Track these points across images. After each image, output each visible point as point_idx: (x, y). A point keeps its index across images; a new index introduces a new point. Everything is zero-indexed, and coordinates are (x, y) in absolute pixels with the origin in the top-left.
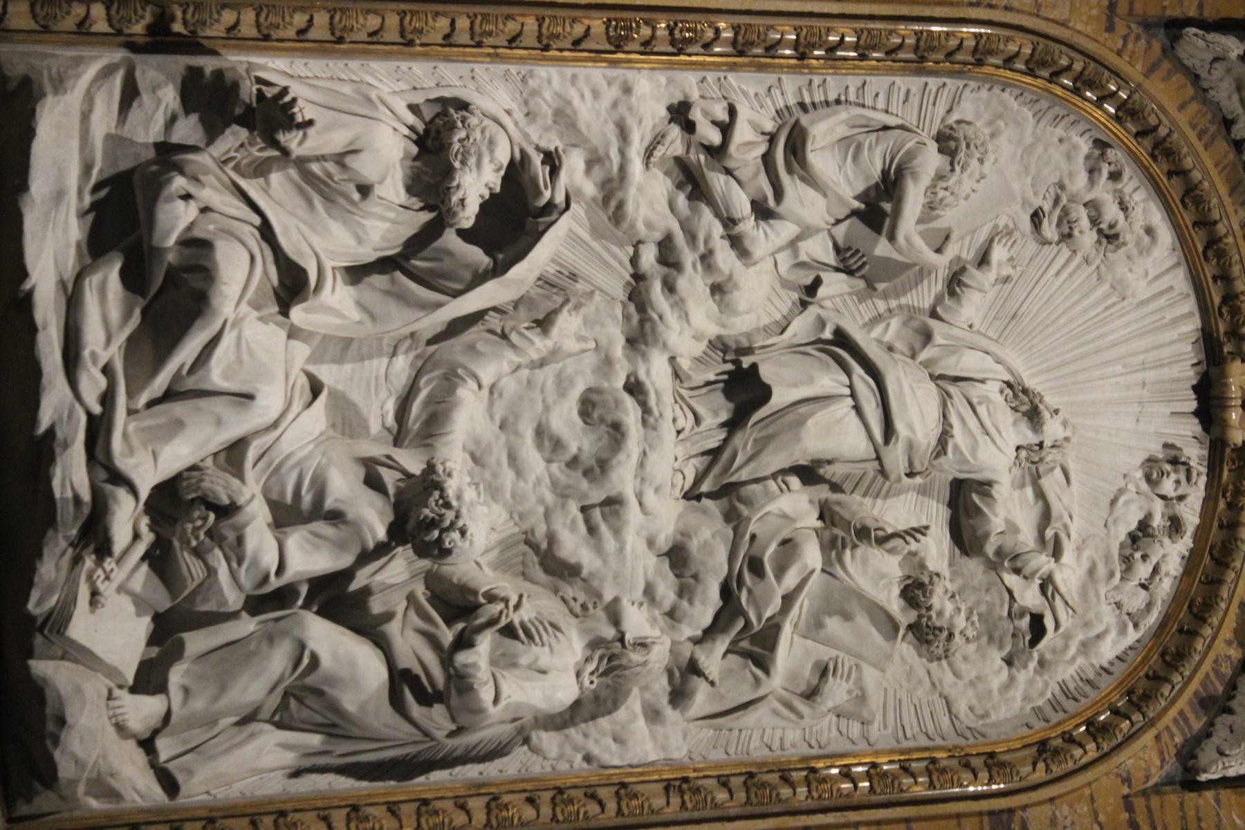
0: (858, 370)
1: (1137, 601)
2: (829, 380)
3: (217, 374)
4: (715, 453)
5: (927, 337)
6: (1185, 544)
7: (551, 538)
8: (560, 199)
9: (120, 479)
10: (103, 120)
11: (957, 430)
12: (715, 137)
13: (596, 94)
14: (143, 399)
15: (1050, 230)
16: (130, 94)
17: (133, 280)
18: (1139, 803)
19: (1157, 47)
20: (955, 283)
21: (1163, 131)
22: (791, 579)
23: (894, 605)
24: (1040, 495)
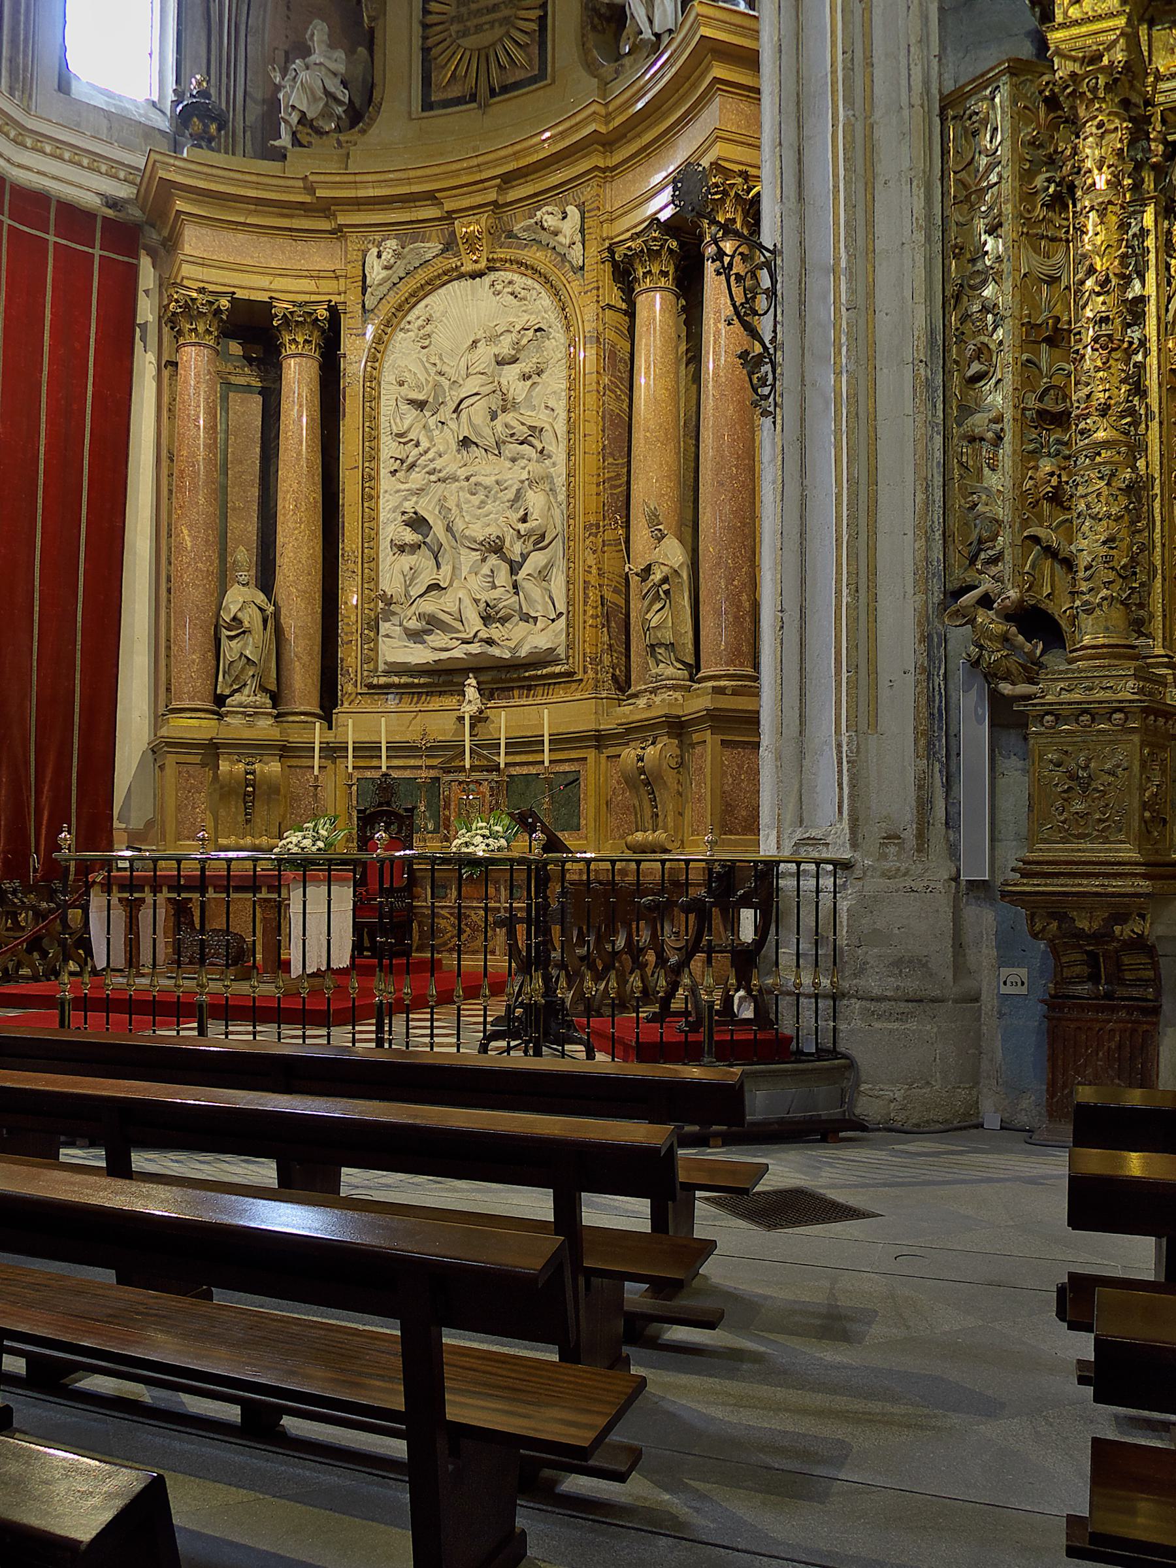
0: (461, 407)
1: (534, 293)
2: (464, 415)
3: (454, 609)
4: (486, 450)
5: (454, 382)
6: (516, 277)
7: (508, 501)
8: (413, 510)
9: (475, 636)
10: (395, 643)
11: (477, 369)
12: (399, 461)
13: (388, 501)
14: (461, 628)
15: (427, 343)
16: (387, 636)
17: (429, 632)
18: (586, 288)
19: (372, 316)
20: (441, 374)
21: (394, 310)
22: (514, 423)
23: (529, 383)
24: (502, 334)
